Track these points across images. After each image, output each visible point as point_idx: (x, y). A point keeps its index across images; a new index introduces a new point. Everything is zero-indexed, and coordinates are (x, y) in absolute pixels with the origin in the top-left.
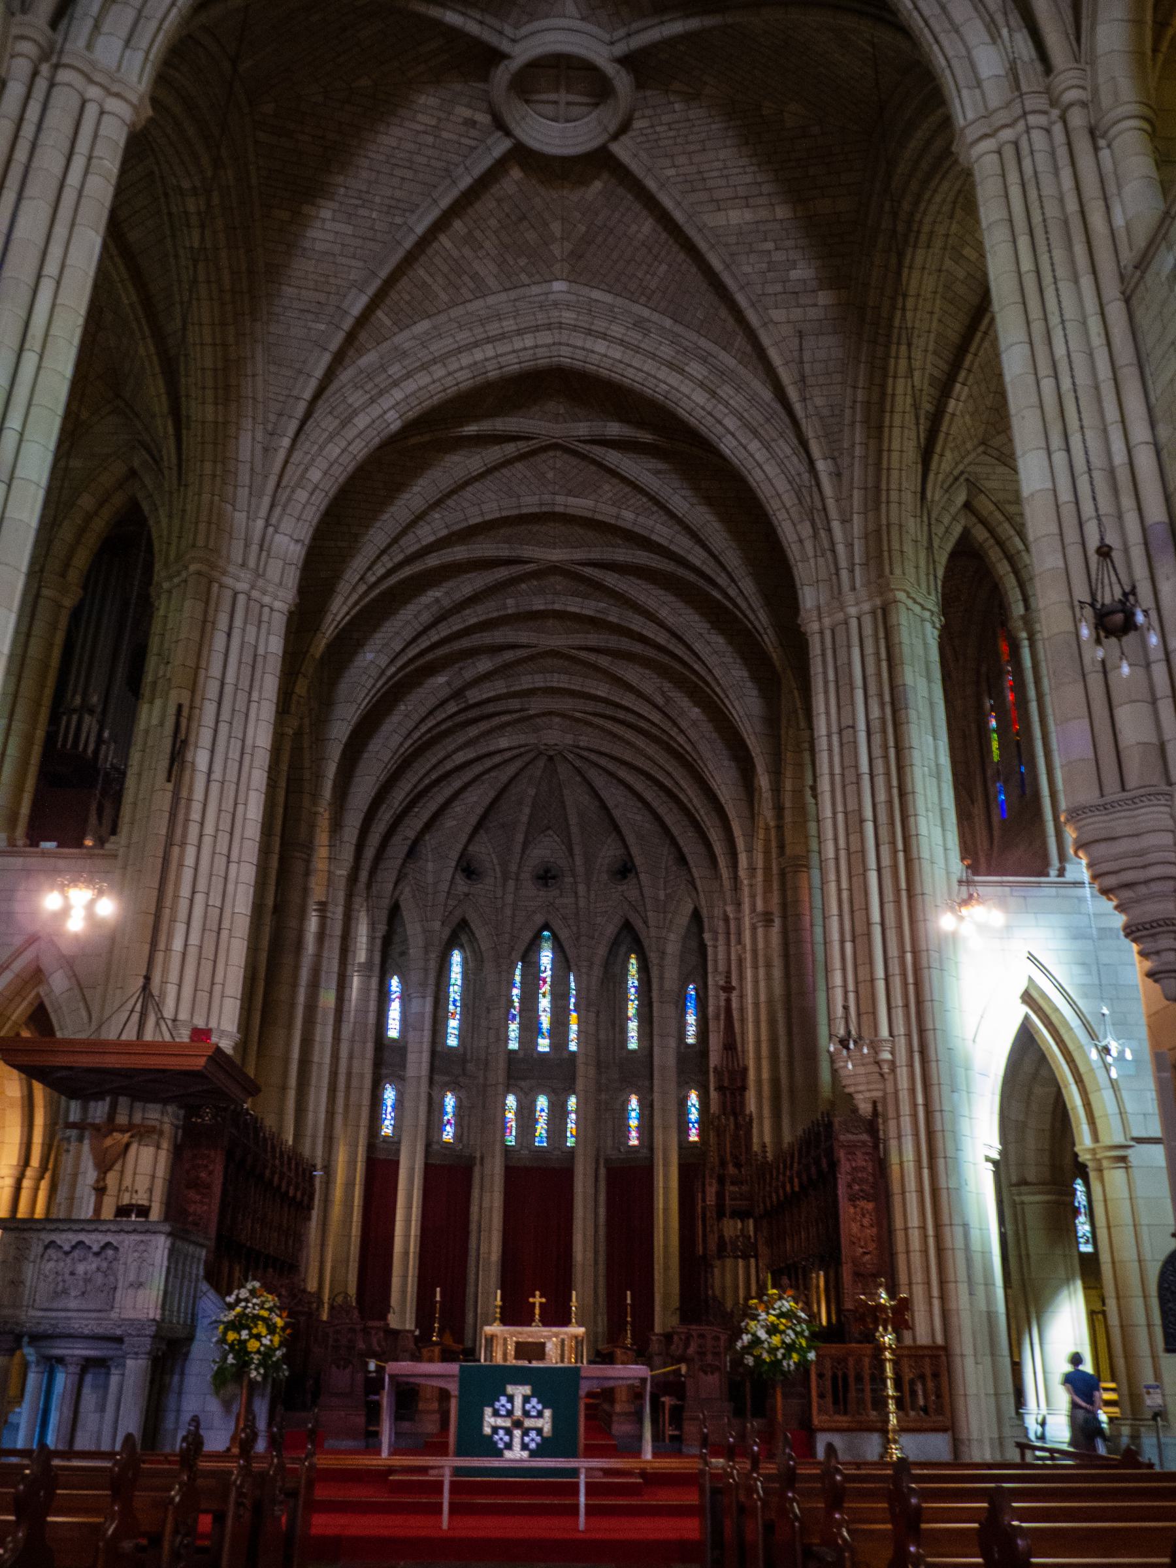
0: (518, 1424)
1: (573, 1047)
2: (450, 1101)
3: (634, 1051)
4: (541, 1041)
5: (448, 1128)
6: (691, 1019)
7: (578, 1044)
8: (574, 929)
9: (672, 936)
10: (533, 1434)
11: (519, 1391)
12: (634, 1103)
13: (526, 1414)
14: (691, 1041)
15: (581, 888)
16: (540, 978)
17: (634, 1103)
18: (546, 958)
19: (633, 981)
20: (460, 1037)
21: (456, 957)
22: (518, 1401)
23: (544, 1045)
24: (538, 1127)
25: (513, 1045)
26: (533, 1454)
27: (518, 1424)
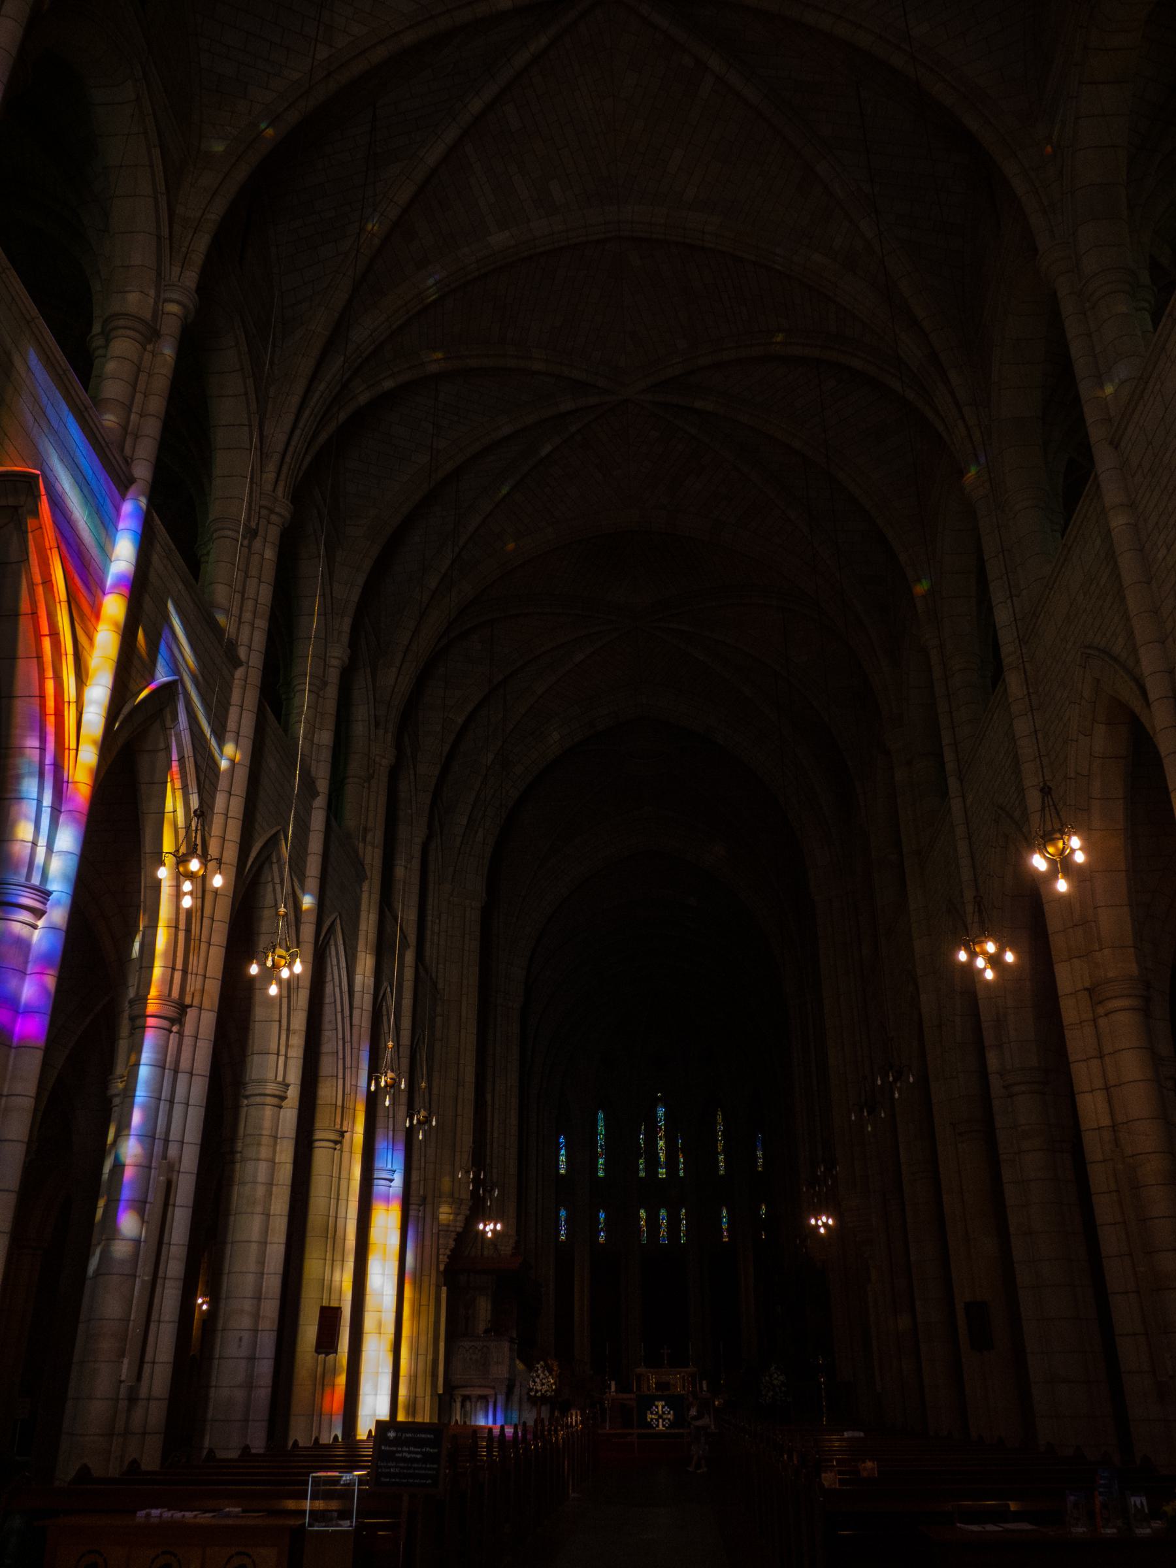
0: (660, 1417)
1: (681, 1174)
2: (602, 1216)
4: (660, 1170)
5: (602, 1234)
6: (760, 1154)
7: (684, 1172)
10: (667, 1421)
11: (660, 1404)
13: (663, 1413)
18: (661, 1112)
19: (719, 1128)
20: (604, 1170)
21: (601, 1115)
22: (660, 1408)
23: (662, 1173)
25: (642, 1174)
26: (667, 1428)
27: (660, 1417)
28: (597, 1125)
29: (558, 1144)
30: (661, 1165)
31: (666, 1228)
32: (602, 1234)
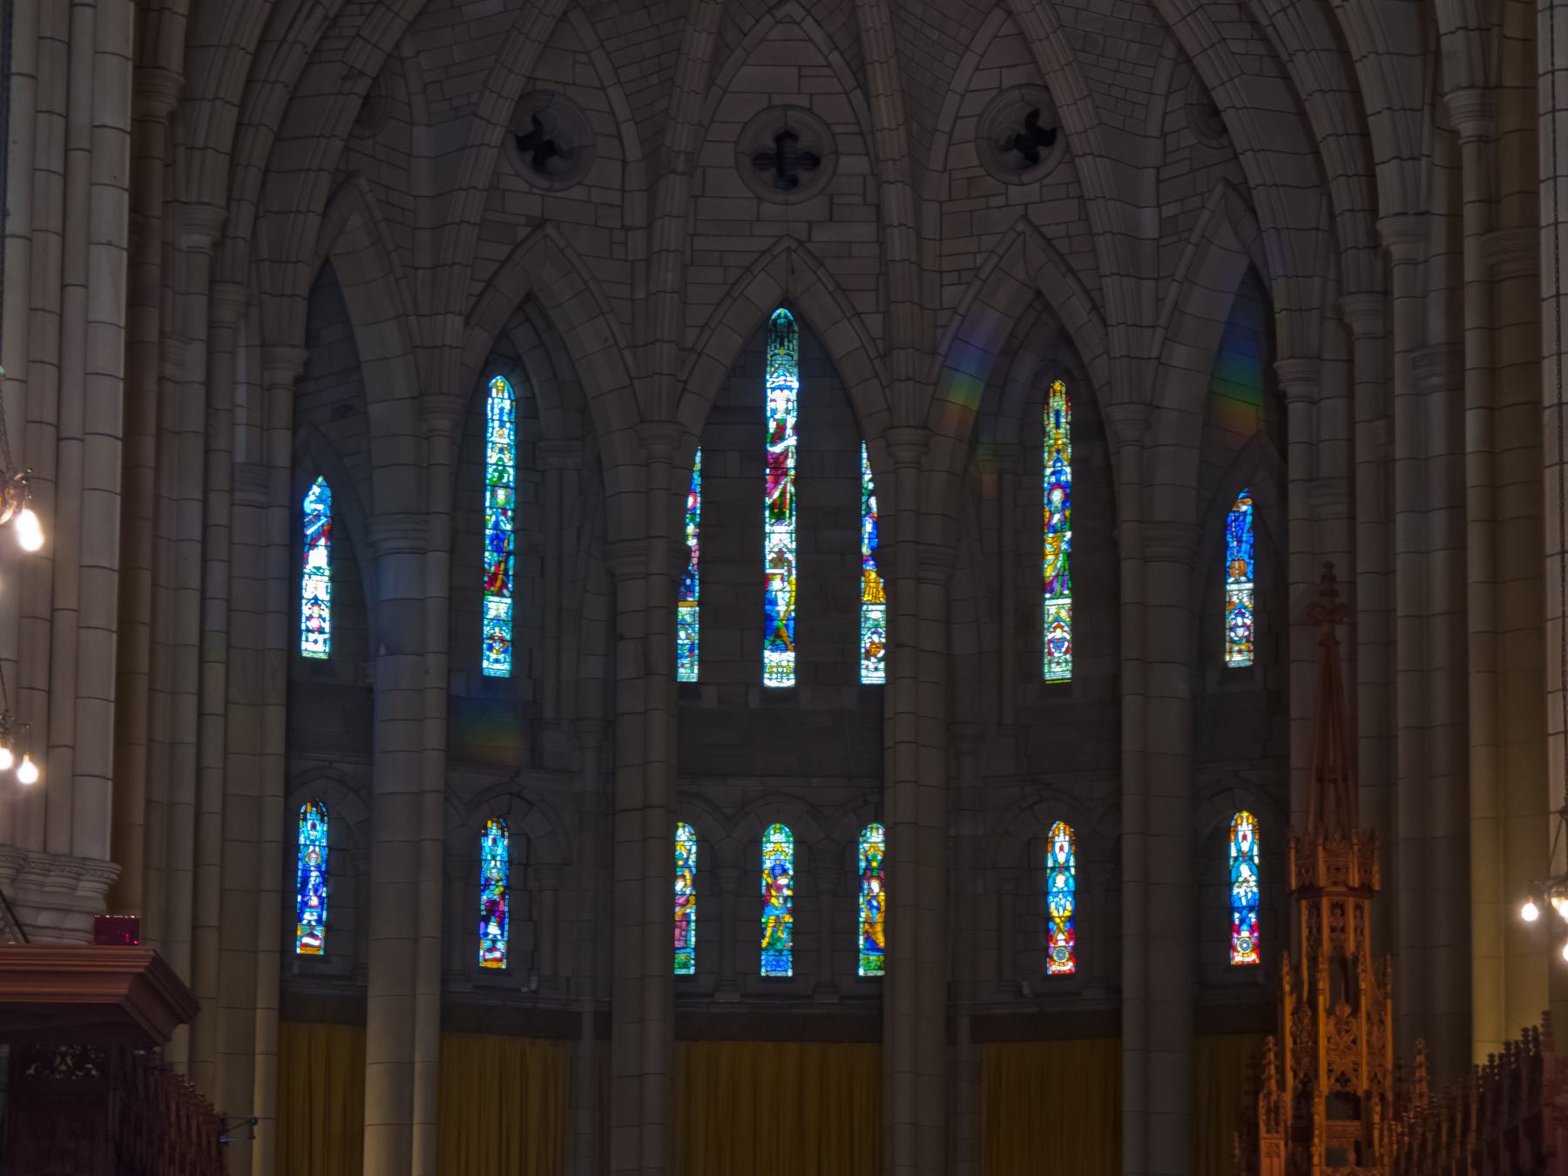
2: (495, 848)
3: (1060, 688)
4: (771, 657)
6: (1240, 591)
8: (875, 323)
9: (1181, 355)
12: (1062, 846)
14: (1237, 658)
15: (896, 200)
16: (763, 458)
17: (1062, 846)
19: (1058, 468)
20: (518, 648)
21: (500, 400)
24: (768, 920)
25: (688, 672)
28: (481, 442)
29: (297, 518)
30: (778, 636)
31: (791, 912)
32: (493, 929)
